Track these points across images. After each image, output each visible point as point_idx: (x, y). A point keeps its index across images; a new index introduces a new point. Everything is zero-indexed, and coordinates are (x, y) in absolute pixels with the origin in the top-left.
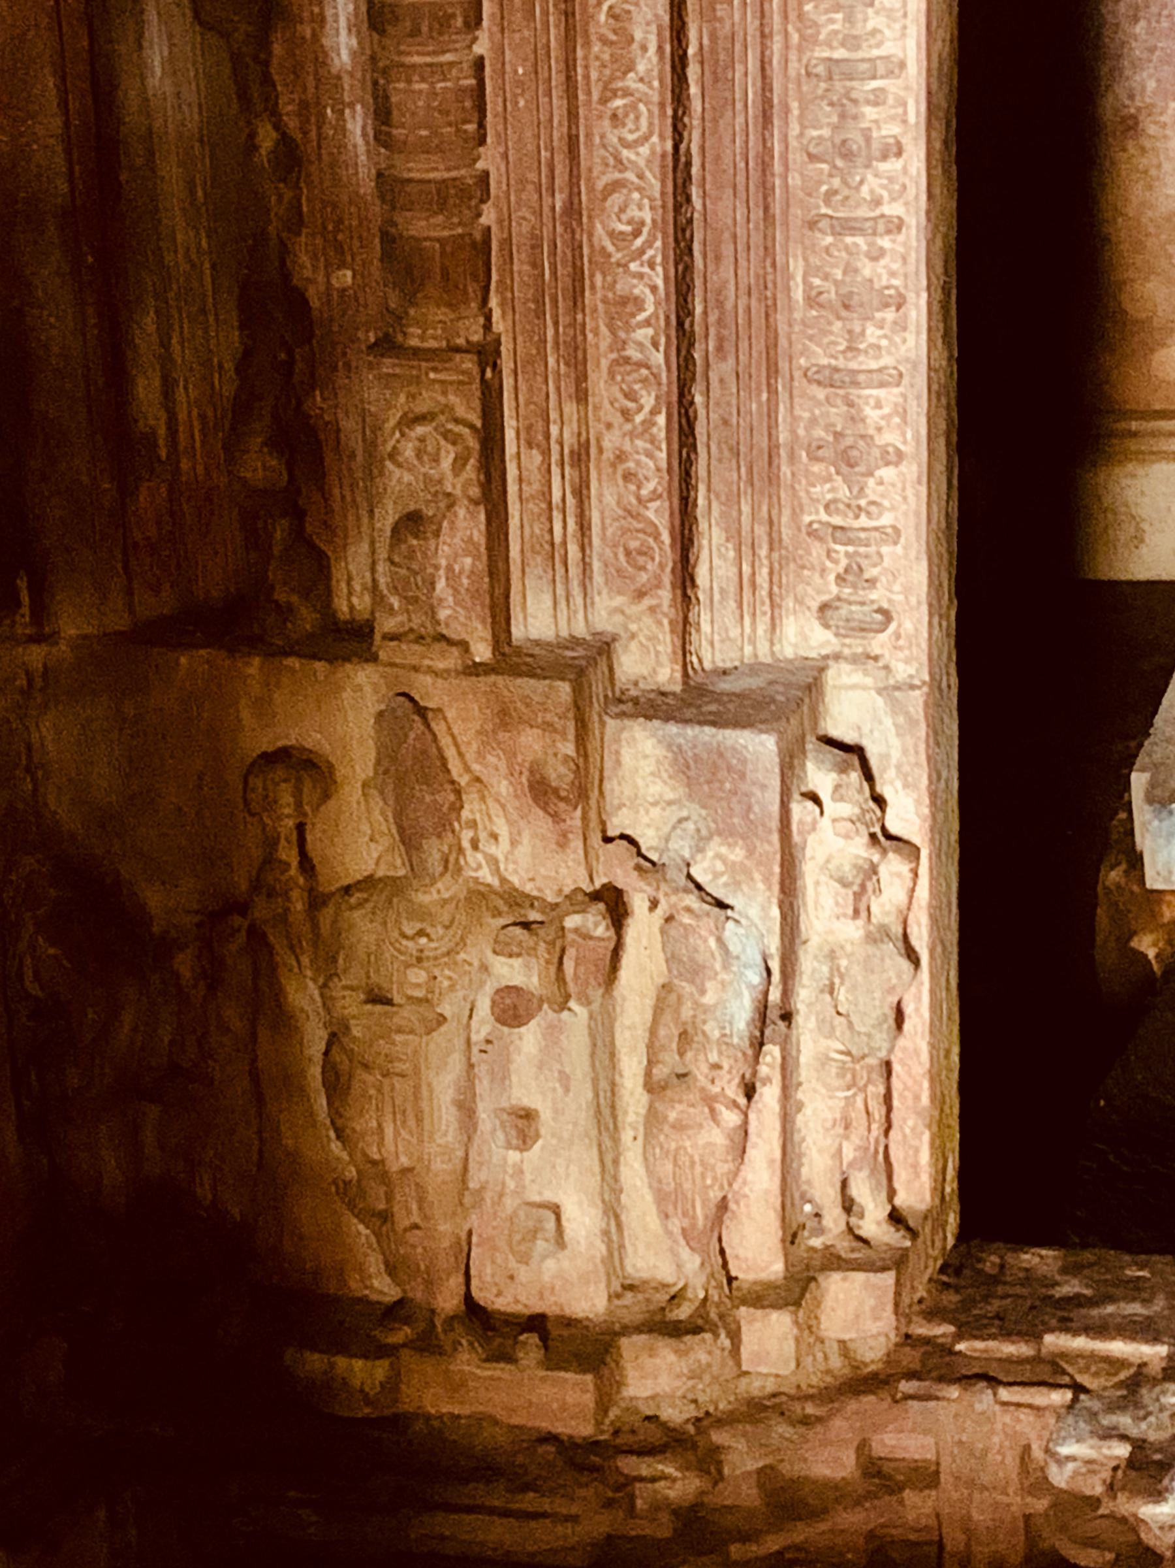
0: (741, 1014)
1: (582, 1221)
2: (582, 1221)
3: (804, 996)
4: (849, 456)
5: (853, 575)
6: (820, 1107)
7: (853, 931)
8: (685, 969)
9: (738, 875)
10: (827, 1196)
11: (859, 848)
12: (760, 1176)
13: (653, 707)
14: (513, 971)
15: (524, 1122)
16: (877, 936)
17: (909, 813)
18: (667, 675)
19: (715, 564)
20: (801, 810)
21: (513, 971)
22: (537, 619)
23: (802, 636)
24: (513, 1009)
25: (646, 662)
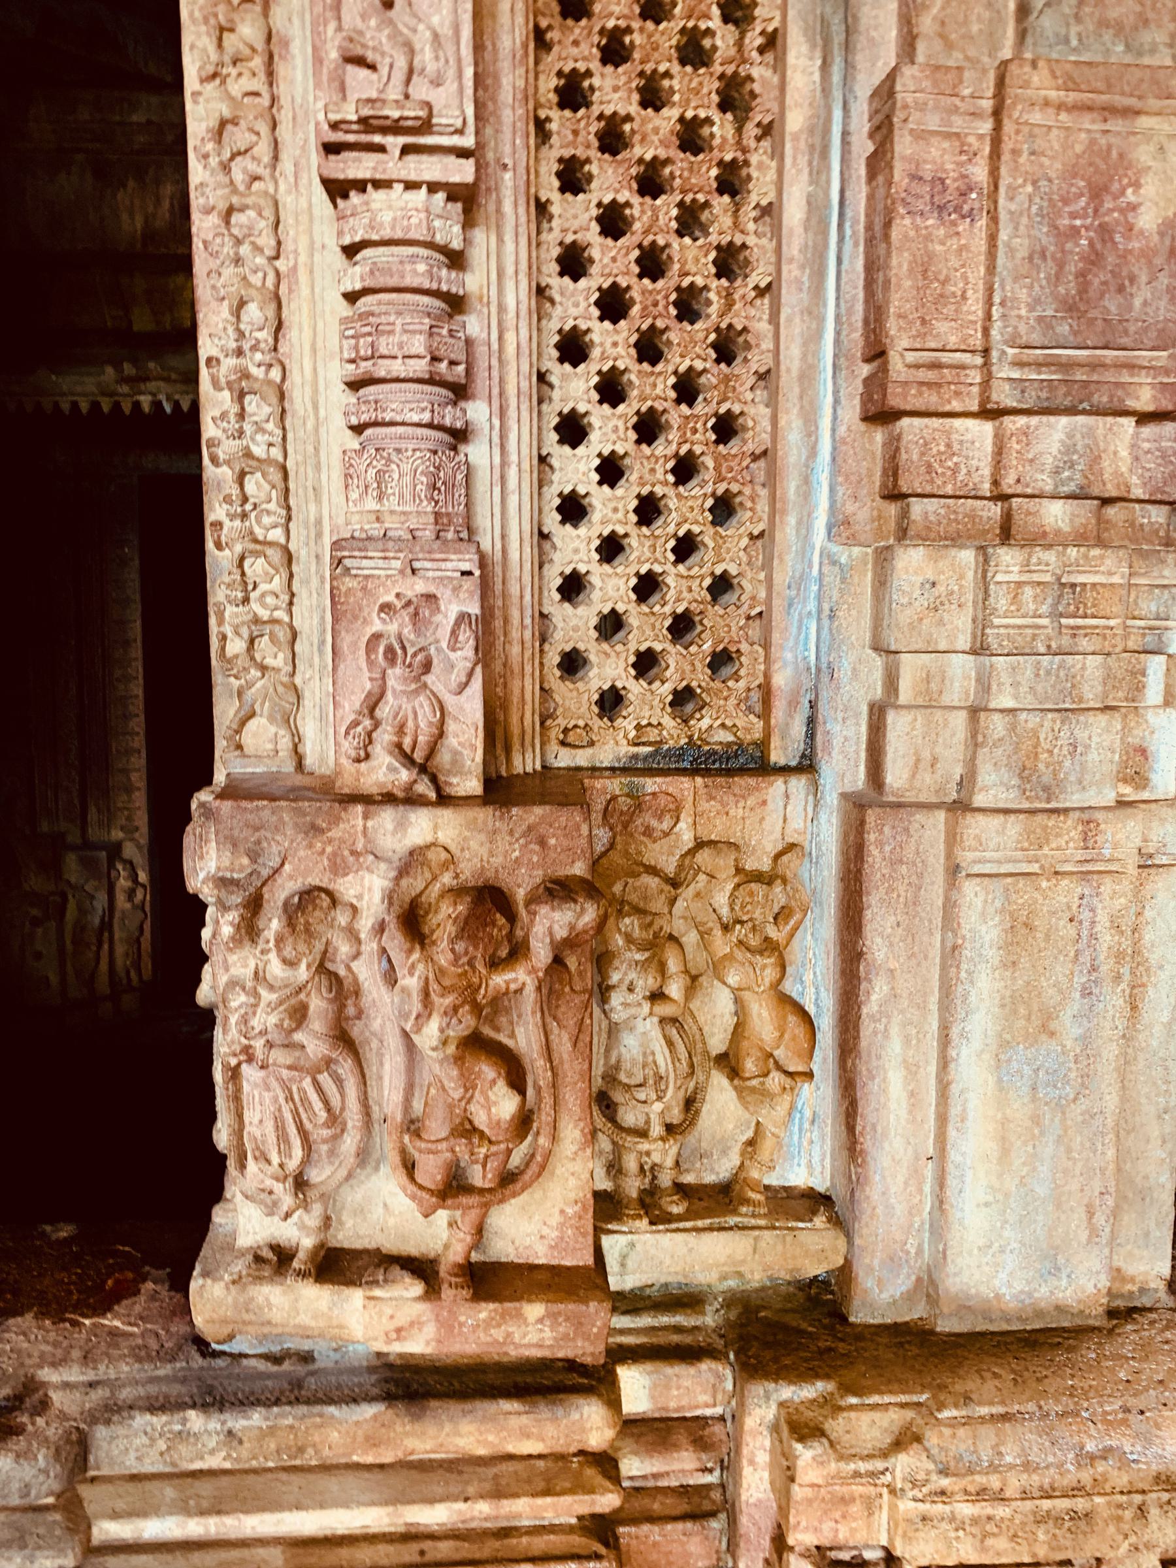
0: (97, 921)
1: (54, 979)
2: (54, 979)
3: (116, 921)
4: (129, 789)
5: (129, 818)
6: (120, 950)
7: (128, 906)
8: (82, 911)
9: (96, 889)
10: (123, 974)
11: (129, 884)
12: (104, 966)
13: (74, 848)
14: (35, 912)
15: (38, 956)
16: (135, 907)
17: (143, 877)
18: (79, 841)
19: (93, 815)
20: (113, 874)
21: (35, 912)
22: (45, 827)
23: (117, 835)
24: (36, 922)
25: (74, 838)
